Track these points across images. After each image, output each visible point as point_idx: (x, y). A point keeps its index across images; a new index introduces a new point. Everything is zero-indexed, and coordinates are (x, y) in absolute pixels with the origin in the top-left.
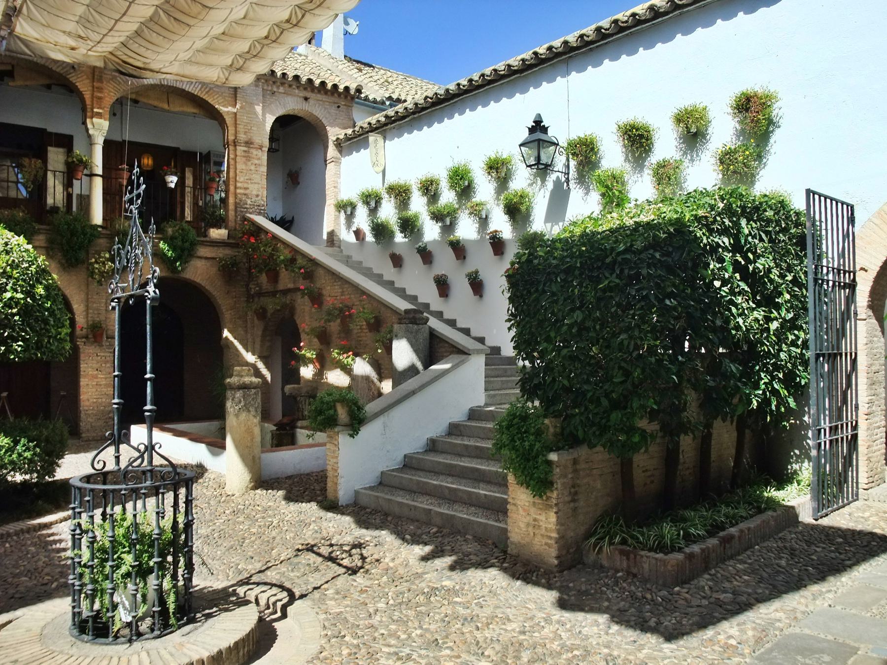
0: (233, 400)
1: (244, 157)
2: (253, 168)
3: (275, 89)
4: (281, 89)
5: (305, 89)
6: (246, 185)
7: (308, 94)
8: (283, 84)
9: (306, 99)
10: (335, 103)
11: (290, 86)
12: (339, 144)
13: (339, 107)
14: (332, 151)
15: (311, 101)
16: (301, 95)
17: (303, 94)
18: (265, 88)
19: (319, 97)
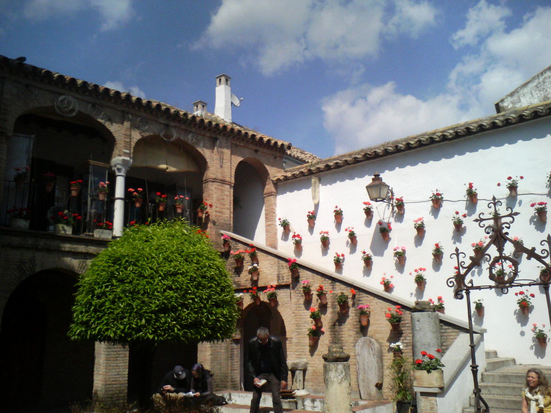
0: (336, 371)
1: (220, 189)
2: (225, 197)
3: (238, 143)
4: (242, 144)
5: (256, 144)
6: (221, 210)
7: (258, 148)
8: (243, 140)
9: (256, 151)
10: (273, 155)
11: (247, 142)
12: (277, 183)
13: (275, 158)
14: (269, 187)
15: (259, 153)
16: (254, 148)
17: (254, 148)
18: (232, 142)
19: (265, 150)
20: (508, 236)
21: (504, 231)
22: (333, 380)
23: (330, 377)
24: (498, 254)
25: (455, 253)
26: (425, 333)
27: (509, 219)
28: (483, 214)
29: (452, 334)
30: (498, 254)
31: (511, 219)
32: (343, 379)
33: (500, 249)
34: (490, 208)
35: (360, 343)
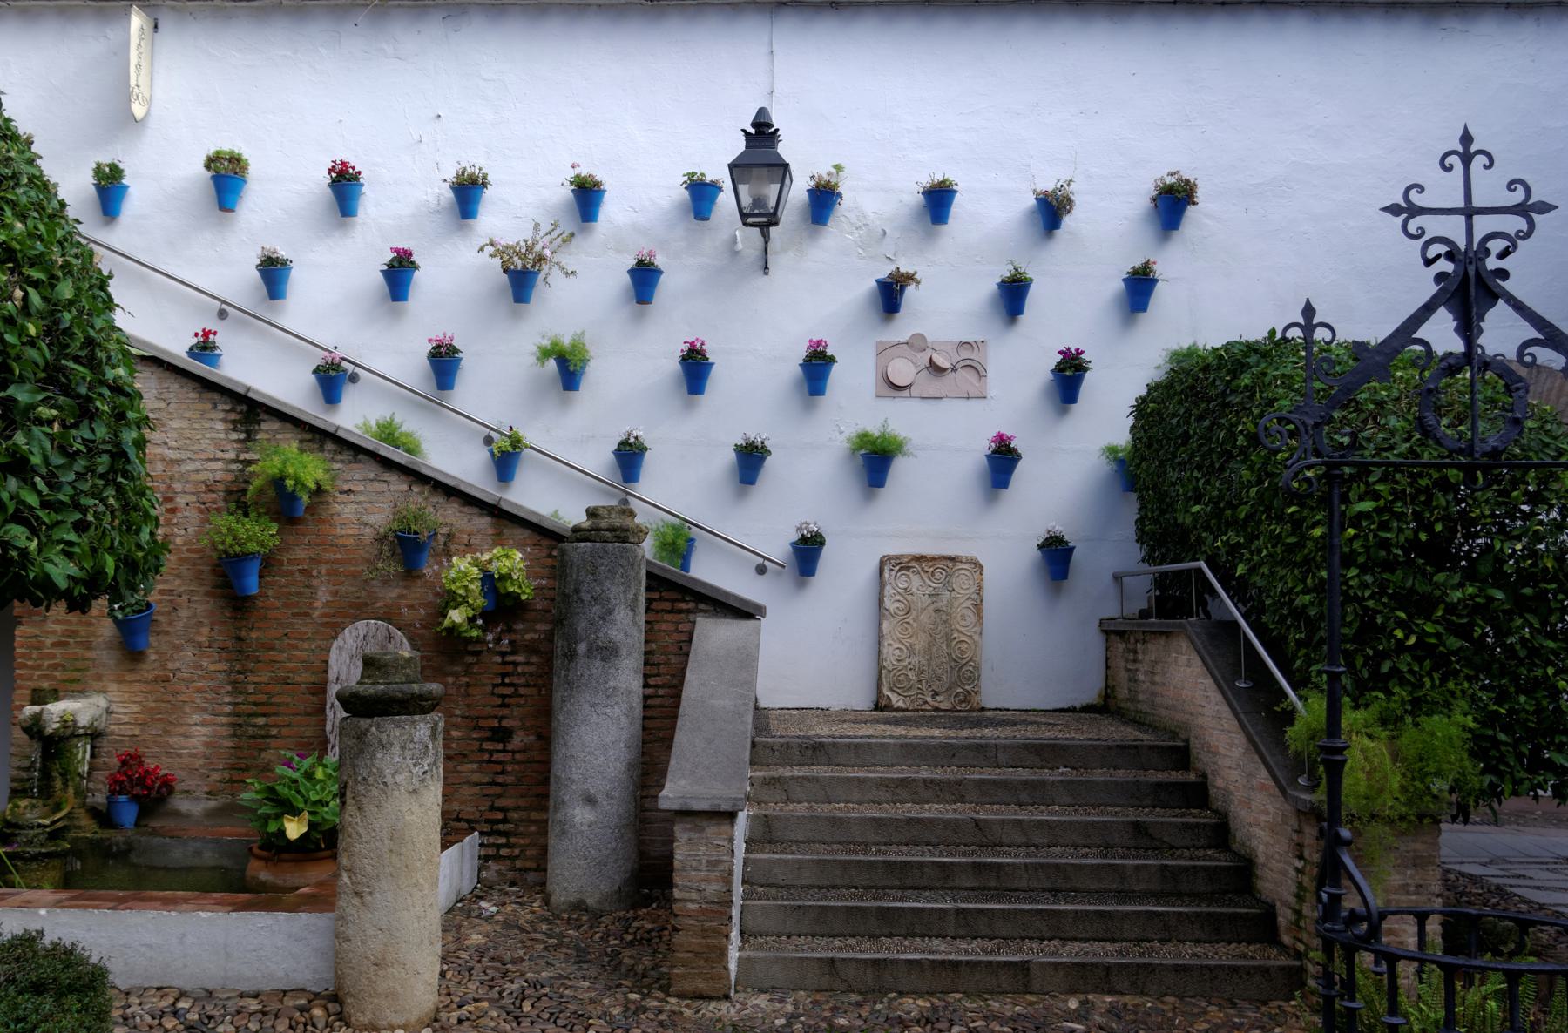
20: (1507, 285)
21: (1492, 263)
22: (389, 780)
23: (381, 772)
24: (1458, 346)
25: (1302, 321)
26: (610, 612)
27: (1514, 224)
28: (1421, 189)
29: (669, 617)
30: (1458, 346)
31: (1518, 223)
32: (428, 776)
33: (1468, 327)
34: (1449, 169)
35: (350, 642)
